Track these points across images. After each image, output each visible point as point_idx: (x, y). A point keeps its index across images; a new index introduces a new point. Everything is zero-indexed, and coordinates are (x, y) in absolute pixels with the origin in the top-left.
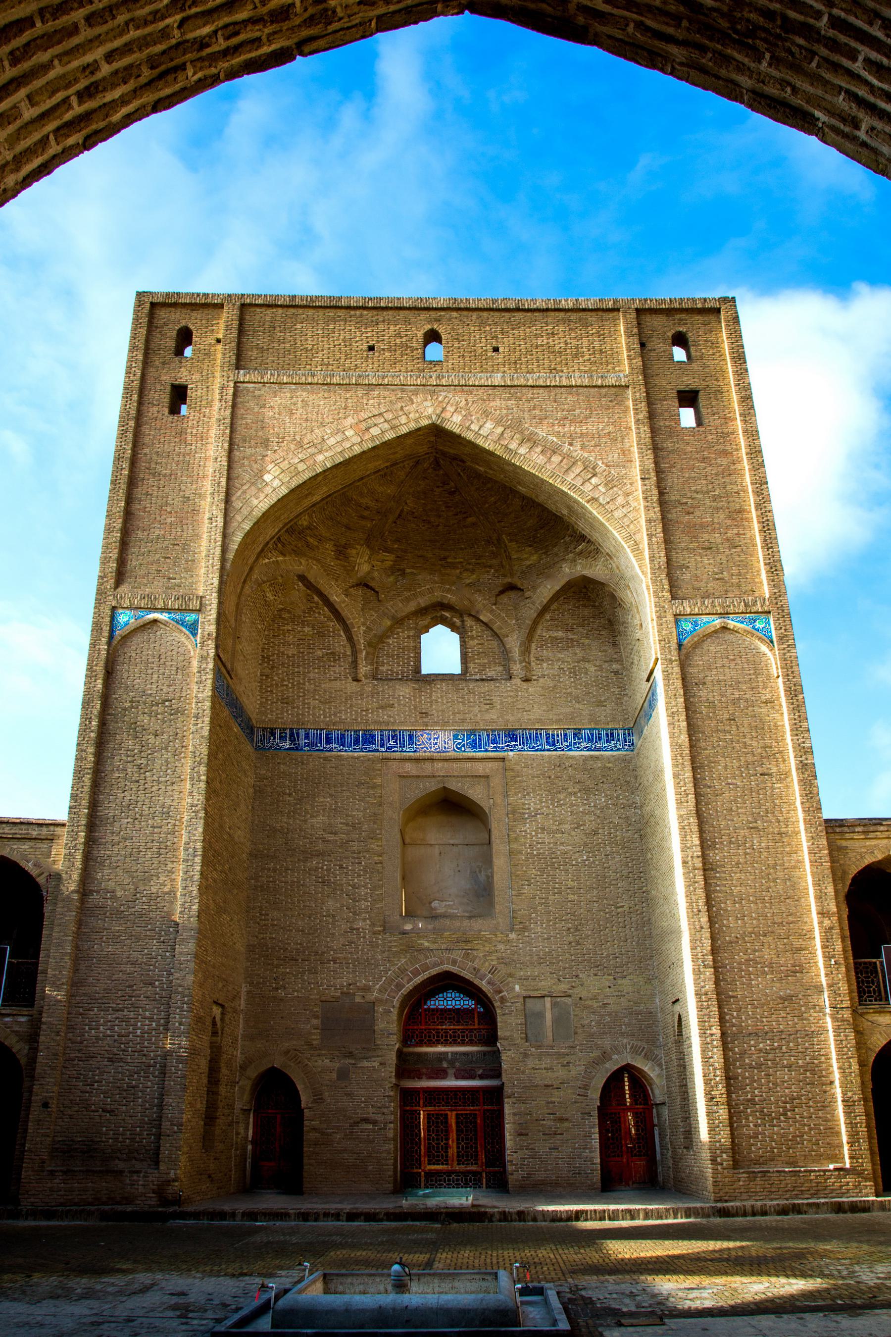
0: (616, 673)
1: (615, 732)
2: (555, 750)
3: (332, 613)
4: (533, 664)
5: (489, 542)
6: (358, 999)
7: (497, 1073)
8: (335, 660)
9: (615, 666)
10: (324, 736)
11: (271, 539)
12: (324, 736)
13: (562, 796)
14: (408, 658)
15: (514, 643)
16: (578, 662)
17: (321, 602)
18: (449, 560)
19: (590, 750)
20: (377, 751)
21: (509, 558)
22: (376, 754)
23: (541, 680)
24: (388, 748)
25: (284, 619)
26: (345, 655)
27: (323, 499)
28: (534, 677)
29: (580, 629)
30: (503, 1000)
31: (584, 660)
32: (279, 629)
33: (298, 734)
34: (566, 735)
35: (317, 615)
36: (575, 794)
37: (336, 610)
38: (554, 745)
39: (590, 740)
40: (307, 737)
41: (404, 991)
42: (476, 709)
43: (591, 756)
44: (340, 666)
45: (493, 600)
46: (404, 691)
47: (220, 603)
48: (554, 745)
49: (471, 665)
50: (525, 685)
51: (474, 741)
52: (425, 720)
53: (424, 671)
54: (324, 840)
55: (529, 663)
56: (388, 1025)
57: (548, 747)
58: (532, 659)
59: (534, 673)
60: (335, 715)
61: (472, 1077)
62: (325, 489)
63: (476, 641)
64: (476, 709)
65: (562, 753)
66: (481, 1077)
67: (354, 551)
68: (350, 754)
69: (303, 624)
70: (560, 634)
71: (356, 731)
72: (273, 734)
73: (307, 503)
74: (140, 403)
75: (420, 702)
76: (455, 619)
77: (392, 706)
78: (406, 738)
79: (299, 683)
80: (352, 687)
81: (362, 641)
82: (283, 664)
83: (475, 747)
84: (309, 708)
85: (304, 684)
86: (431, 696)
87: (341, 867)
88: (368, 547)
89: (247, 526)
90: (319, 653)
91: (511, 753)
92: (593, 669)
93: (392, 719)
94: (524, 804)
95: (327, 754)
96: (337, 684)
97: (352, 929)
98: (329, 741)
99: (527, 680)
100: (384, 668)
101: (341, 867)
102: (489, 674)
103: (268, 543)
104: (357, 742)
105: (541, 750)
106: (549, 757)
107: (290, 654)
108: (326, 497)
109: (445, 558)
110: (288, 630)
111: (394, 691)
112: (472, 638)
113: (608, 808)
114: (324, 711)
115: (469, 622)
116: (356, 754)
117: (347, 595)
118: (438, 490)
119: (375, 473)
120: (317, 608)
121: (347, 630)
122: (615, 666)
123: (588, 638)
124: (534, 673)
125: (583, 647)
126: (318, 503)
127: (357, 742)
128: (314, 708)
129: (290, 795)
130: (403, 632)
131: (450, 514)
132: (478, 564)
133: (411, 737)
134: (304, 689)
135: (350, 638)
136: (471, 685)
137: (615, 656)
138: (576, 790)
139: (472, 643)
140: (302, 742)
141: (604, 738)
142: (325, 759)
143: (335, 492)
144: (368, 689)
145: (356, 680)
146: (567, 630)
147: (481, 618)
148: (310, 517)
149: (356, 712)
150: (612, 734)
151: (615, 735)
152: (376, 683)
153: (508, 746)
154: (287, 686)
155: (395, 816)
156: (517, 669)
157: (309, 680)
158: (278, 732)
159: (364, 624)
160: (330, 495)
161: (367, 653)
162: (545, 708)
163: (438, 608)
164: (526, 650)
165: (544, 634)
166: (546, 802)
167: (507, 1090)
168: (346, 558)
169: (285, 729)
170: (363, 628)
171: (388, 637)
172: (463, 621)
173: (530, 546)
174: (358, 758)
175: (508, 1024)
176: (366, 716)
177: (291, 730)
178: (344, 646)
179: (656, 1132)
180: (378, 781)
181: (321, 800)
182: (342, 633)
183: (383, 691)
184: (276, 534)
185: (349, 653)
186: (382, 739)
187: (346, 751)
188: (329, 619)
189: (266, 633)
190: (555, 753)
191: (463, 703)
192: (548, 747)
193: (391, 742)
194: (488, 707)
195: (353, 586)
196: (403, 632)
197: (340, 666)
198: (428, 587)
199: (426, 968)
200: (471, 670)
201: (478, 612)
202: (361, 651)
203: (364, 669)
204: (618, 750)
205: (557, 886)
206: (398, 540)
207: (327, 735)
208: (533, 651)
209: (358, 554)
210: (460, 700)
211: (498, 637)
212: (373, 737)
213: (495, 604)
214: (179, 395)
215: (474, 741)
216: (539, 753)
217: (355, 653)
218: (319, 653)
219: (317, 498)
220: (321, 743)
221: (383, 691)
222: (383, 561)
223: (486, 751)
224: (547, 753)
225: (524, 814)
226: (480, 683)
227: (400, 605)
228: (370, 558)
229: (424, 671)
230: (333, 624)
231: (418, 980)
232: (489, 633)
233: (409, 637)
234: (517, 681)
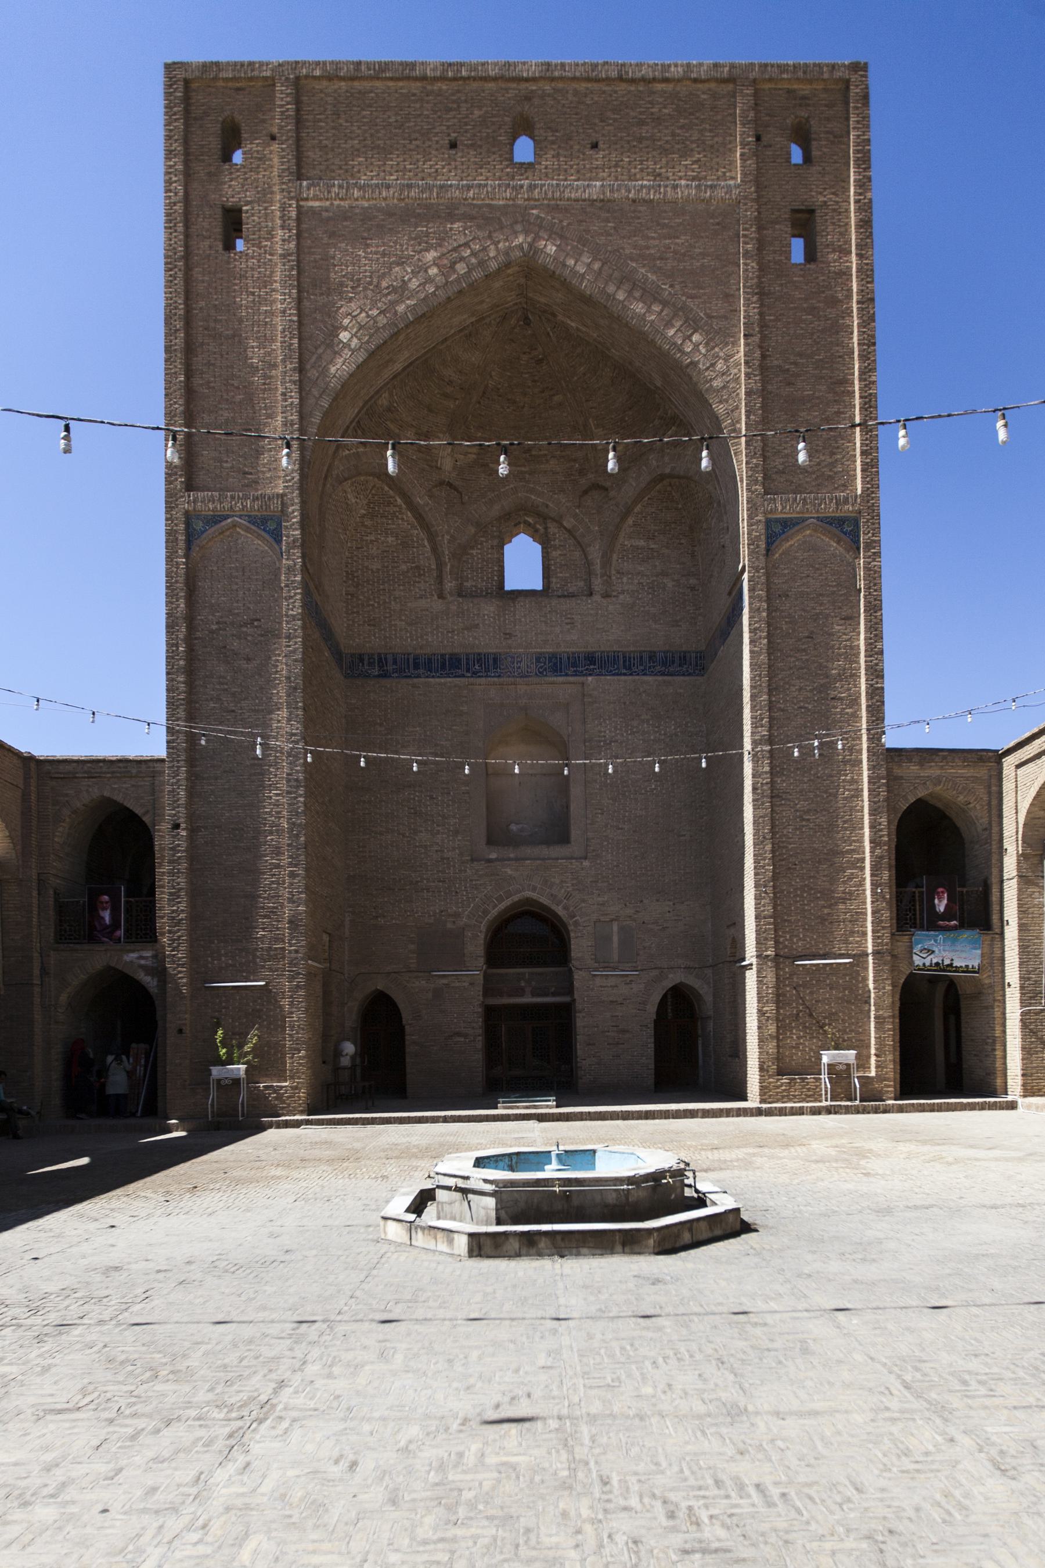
0: (693, 588)
1: (688, 655)
2: (631, 674)
3: (416, 519)
4: (614, 578)
6: (449, 926)
7: (570, 990)
8: (420, 575)
9: (693, 581)
10: (411, 661)
11: (351, 423)
12: (411, 661)
13: (635, 723)
14: (492, 572)
15: (595, 552)
16: (657, 576)
18: (534, 453)
19: (663, 674)
20: (463, 676)
22: (463, 679)
23: (621, 597)
24: (474, 673)
25: (366, 526)
27: (404, 369)
28: (615, 594)
30: (576, 923)
31: (664, 574)
32: (362, 540)
33: (386, 659)
34: (641, 657)
36: (648, 721)
37: (420, 515)
38: (630, 668)
39: (664, 664)
40: (395, 662)
41: (490, 917)
42: (558, 630)
43: (664, 682)
44: (426, 582)
46: (489, 608)
47: (303, 503)
48: (630, 668)
49: (554, 580)
51: (555, 664)
52: (510, 642)
53: (508, 587)
55: (610, 577)
56: (476, 947)
57: (624, 671)
58: (613, 572)
59: (614, 588)
60: (422, 637)
61: (546, 995)
62: (406, 354)
63: (559, 552)
64: (558, 630)
65: (637, 677)
66: (554, 994)
68: (437, 680)
69: (387, 534)
70: (642, 543)
71: (443, 655)
72: (361, 660)
73: (387, 374)
74: (187, 236)
75: (504, 621)
76: (538, 526)
77: (477, 626)
78: (491, 662)
79: (385, 602)
80: (438, 605)
81: (447, 552)
82: (368, 581)
83: (556, 671)
84: (396, 630)
85: (390, 603)
86: (514, 615)
87: (431, 798)
89: (325, 403)
90: (404, 567)
91: (590, 678)
92: (670, 584)
93: (477, 642)
94: (600, 732)
95: (416, 680)
96: (423, 603)
97: (443, 859)
98: (416, 666)
99: (606, 596)
100: (468, 584)
101: (431, 798)
102: (571, 590)
103: (348, 427)
104: (443, 667)
105: (618, 674)
106: (625, 681)
107: (374, 567)
108: (408, 366)
110: (371, 541)
111: (479, 610)
112: (555, 548)
113: (676, 735)
114: (411, 633)
115: (553, 529)
116: (443, 680)
117: (430, 497)
118: (525, 357)
119: (461, 331)
121: (432, 537)
122: (693, 581)
123: (668, 548)
124: (614, 588)
126: (399, 374)
127: (443, 667)
128: (401, 630)
129: (381, 725)
130: (487, 542)
132: (563, 457)
133: (495, 660)
134: (390, 608)
135: (434, 550)
136: (554, 602)
137: (693, 569)
138: (648, 717)
139: (555, 554)
140: (390, 668)
141: (677, 661)
142: (414, 686)
143: (416, 360)
144: (454, 608)
145: (441, 596)
147: (565, 524)
148: (391, 395)
149: (442, 633)
150: (685, 657)
151: (688, 659)
152: (460, 600)
154: (373, 605)
156: (597, 584)
157: (395, 598)
158: (366, 658)
159: (448, 533)
160: (411, 364)
161: (452, 566)
162: (623, 628)
163: (521, 513)
164: (606, 562)
166: (621, 730)
167: (579, 1006)
169: (373, 654)
170: (447, 537)
171: (472, 548)
172: (546, 528)
174: (445, 684)
175: (580, 947)
176: (452, 638)
177: (379, 654)
178: (429, 559)
179: (700, 1042)
180: (465, 708)
181: (411, 729)
182: (426, 543)
183: (468, 610)
184: (356, 416)
185: (434, 567)
186: (468, 664)
187: (433, 677)
188: (413, 527)
189: (349, 544)
190: (630, 677)
191: (546, 623)
192: (624, 671)
194: (569, 627)
195: (436, 486)
196: (487, 542)
197: (426, 582)
198: (512, 486)
199: (509, 895)
200: (553, 585)
201: (561, 517)
202: (446, 565)
203: (449, 585)
204: (690, 675)
207: (414, 659)
208: (614, 562)
210: (543, 619)
211: (581, 546)
212: (459, 660)
213: (579, 507)
214: (233, 223)
215: (555, 664)
216: (616, 678)
217: (440, 566)
219: (398, 366)
220: (408, 668)
221: (468, 610)
223: (567, 675)
224: (623, 678)
225: (600, 741)
226: (562, 600)
227: (484, 508)
229: (508, 587)
230: (417, 532)
231: (502, 906)
232: (572, 541)
233: (492, 547)
234: (597, 598)
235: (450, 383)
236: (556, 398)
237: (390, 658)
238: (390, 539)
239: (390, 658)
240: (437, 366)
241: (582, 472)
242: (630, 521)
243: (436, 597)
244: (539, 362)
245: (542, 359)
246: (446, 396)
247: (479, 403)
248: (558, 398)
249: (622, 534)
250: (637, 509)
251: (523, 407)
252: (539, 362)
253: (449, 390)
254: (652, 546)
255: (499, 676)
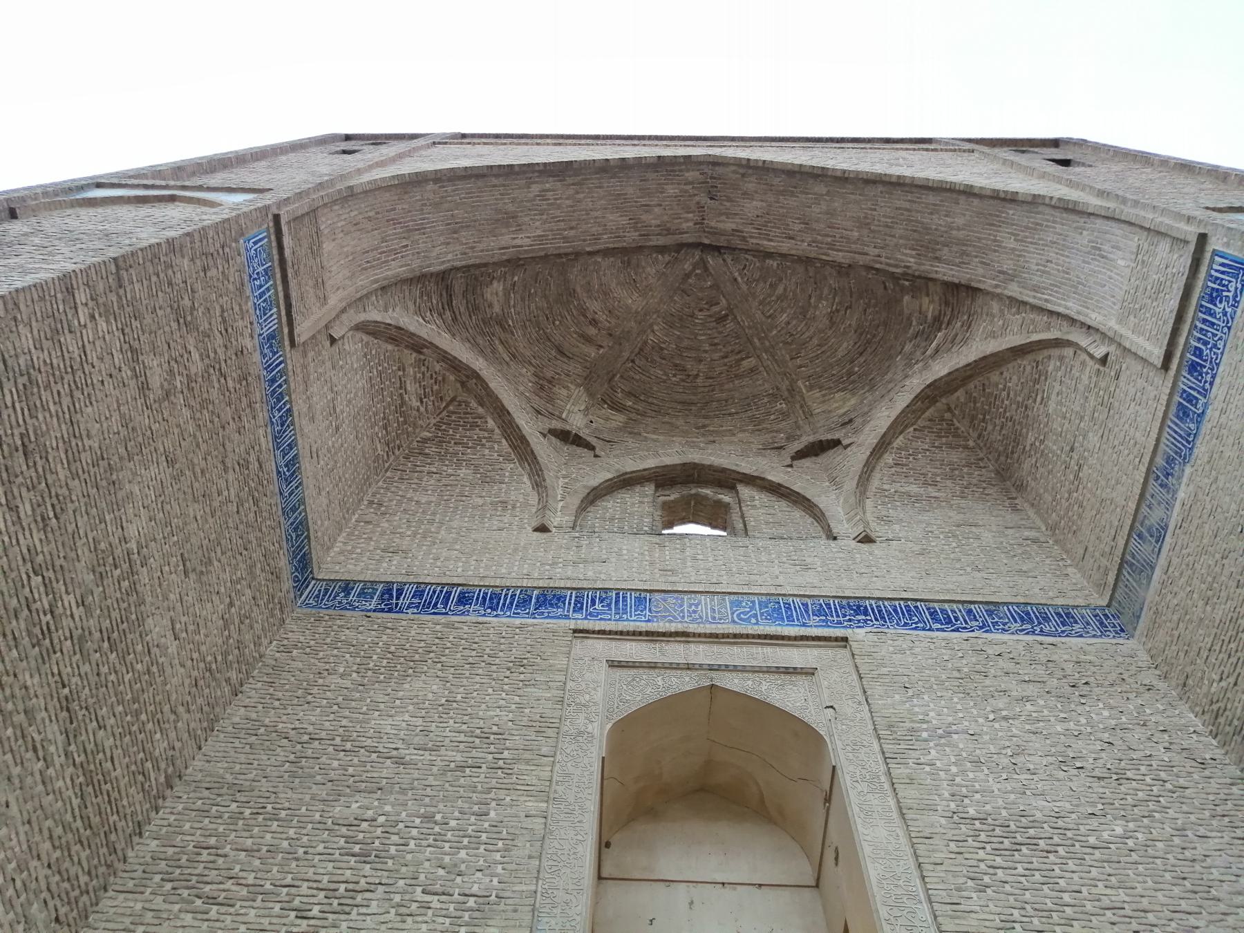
5: (774, 397)
17: (497, 431)
21: (809, 415)
26: (526, 504)
29: (949, 483)
35: (487, 452)
45: (789, 461)
50: (865, 547)
54: (400, 761)
67: (564, 392)
70: (914, 489)
88: (587, 390)
109: (704, 426)
116: (518, 621)
120: (489, 439)
125: (960, 510)
131: (716, 356)
146: (926, 484)
153: (850, 620)
155: (594, 728)
165: (886, 487)
168: (550, 400)
173: (843, 390)
193: (598, 606)
205: (1067, 898)
206: (630, 394)
209: (569, 397)
218: (480, 501)
222: (607, 419)
228: (587, 409)
235: (594, 322)
236: (745, 363)
237: (409, 591)
238: (463, 472)
239: (409, 591)
240: (578, 290)
241: (791, 438)
242: (889, 458)
243: (530, 529)
244: (721, 319)
245: (726, 315)
246: (588, 340)
247: (633, 361)
248: (746, 364)
249: (877, 475)
250: (899, 441)
251: (697, 376)
252: (721, 319)
253: (592, 331)
254: (934, 494)
255: (649, 621)
